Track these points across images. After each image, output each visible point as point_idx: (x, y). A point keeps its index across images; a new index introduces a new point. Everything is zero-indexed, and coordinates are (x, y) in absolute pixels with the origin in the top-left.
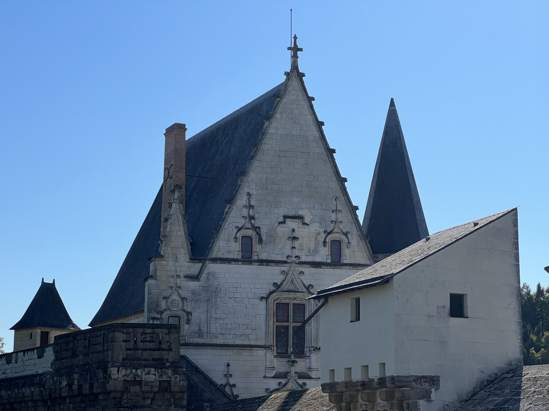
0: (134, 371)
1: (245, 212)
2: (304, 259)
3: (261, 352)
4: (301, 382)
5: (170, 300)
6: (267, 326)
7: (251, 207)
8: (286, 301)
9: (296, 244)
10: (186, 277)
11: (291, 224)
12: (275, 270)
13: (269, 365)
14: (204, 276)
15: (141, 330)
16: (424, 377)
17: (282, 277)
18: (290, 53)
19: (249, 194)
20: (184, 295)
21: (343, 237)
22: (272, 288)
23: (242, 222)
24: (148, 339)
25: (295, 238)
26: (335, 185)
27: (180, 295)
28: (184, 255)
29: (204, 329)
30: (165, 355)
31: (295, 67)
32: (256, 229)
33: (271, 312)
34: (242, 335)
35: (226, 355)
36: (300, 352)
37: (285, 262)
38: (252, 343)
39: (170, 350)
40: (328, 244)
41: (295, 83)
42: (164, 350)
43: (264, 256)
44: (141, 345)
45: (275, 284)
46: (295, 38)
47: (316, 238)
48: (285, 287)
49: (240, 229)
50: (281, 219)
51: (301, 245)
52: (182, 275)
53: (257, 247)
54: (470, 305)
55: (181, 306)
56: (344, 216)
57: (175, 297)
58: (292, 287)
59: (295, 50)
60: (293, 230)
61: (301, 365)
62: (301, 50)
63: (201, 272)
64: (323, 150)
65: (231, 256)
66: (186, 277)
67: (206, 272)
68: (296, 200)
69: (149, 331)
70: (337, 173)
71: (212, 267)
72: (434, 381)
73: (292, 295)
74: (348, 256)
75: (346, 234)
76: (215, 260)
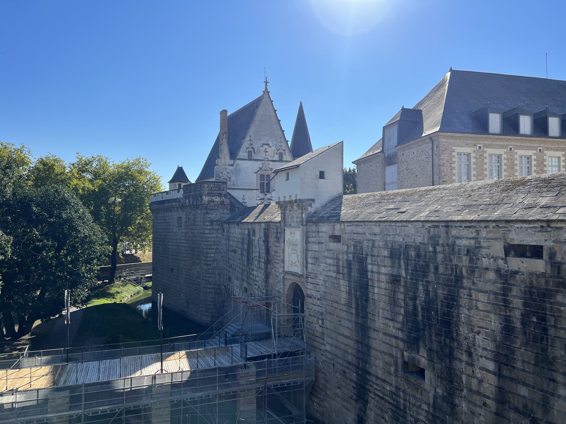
0: (211, 197)
2: (269, 159)
3: (255, 191)
4: (269, 201)
5: (223, 173)
6: (257, 182)
7: (252, 140)
8: (264, 174)
9: (267, 154)
10: (228, 165)
11: (265, 147)
12: (260, 163)
13: (258, 196)
14: (235, 165)
15: (213, 183)
16: (310, 199)
18: (265, 84)
19: (250, 136)
20: (228, 171)
21: (283, 152)
22: (259, 169)
23: (248, 146)
24: (216, 186)
25: (267, 152)
26: (280, 133)
27: (226, 171)
28: (228, 158)
29: (235, 183)
30: (222, 192)
31: (266, 89)
32: (253, 148)
33: (258, 178)
34: (248, 185)
35: (242, 193)
36: (268, 191)
37: (263, 160)
38: (252, 188)
39: (223, 190)
40: (278, 154)
41: (266, 95)
42: (221, 190)
43: (256, 158)
44: (213, 189)
45: (260, 168)
46: (266, 78)
47: (274, 152)
48: (263, 169)
49: (247, 148)
50: (262, 145)
51: (268, 154)
53: (253, 155)
54: (326, 175)
55: (227, 175)
56: (283, 144)
57: (225, 172)
58: (265, 169)
59: (266, 82)
60: (266, 149)
61: (269, 196)
63: (234, 163)
65: (244, 158)
66: (228, 165)
67: (236, 163)
68: (267, 138)
69: (216, 184)
71: (238, 162)
72: (313, 200)
73: (265, 172)
74: (285, 158)
75: (284, 150)
76: (239, 159)
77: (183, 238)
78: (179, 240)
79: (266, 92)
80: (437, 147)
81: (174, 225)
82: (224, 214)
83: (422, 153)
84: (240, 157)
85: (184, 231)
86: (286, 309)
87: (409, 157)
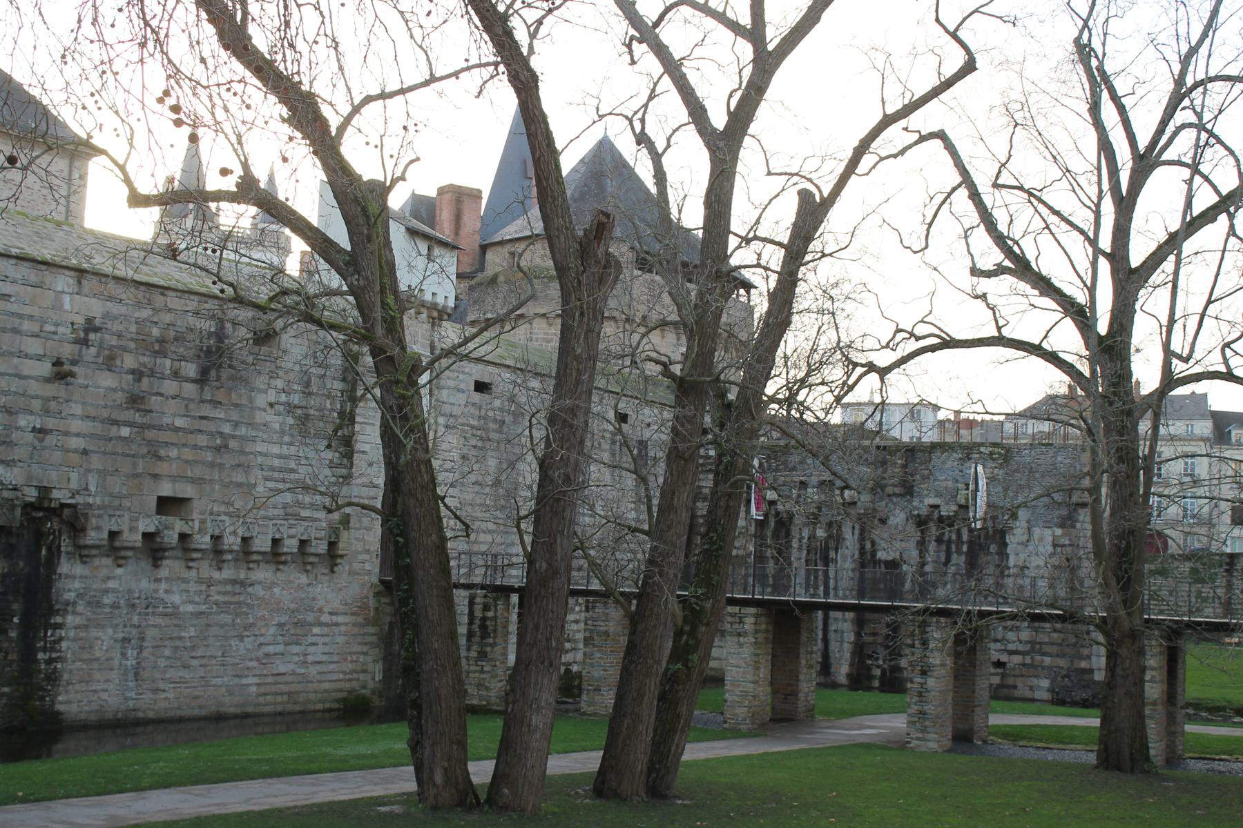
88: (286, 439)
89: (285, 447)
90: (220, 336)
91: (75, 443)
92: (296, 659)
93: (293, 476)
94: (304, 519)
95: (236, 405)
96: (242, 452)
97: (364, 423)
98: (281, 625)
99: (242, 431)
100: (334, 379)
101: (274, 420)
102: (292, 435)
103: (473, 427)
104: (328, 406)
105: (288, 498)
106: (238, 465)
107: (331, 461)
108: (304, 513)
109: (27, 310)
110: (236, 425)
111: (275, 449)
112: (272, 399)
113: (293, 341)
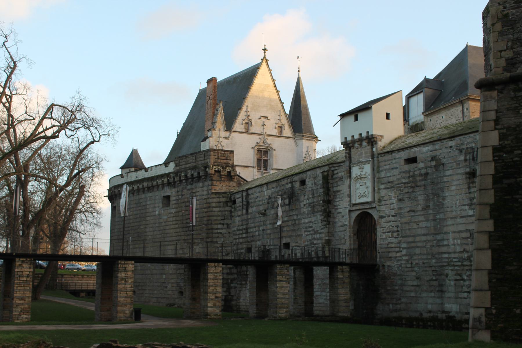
1: (245, 114)
3: (252, 169)
7: (248, 111)
9: (265, 127)
11: (263, 119)
12: (258, 137)
14: (231, 137)
17: (260, 140)
22: (256, 144)
23: (244, 118)
26: (280, 105)
28: (222, 128)
31: (265, 56)
39: (231, 160)
41: (264, 64)
42: (228, 160)
46: (265, 45)
52: (222, 137)
54: (391, 117)
59: (265, 50)
62: (267, 50)
64: (275, 91)
69: (223, 152)
70: (281, 100)
71: (233, 134)
72: (382, 136)
77: (171, 219)
78: (165, 222)
79: (265, 59)
80: (467, 109)
81: (155, 207)
82: (230, 186)
83: (451, 116)
84: (237, 130)
85: (173, 211)
86: (352, 239)
87: (437, 122)
88: (309, 216)
89: (309, 219)
90: (293, 187)
91: (269, 232)
92: (324, 298)
93: (311, 229)
94: (316, 244)
95: (297, 209)
96: (299, 224)
97: (340, 201)
98: (320, 285)
99: (299, 217)
100: (320, 188)
101: (305, 210)
102: (310, 214)
103: (405, 183)
104: (319, 199)
105: (310, 237)
106: (298, 229)
107: (321, 220)
108: (315, 242)
109: (261, 199)
110: (297, 215)
111: (307, 221)
112: (305, 203)
113: (309, 180)
